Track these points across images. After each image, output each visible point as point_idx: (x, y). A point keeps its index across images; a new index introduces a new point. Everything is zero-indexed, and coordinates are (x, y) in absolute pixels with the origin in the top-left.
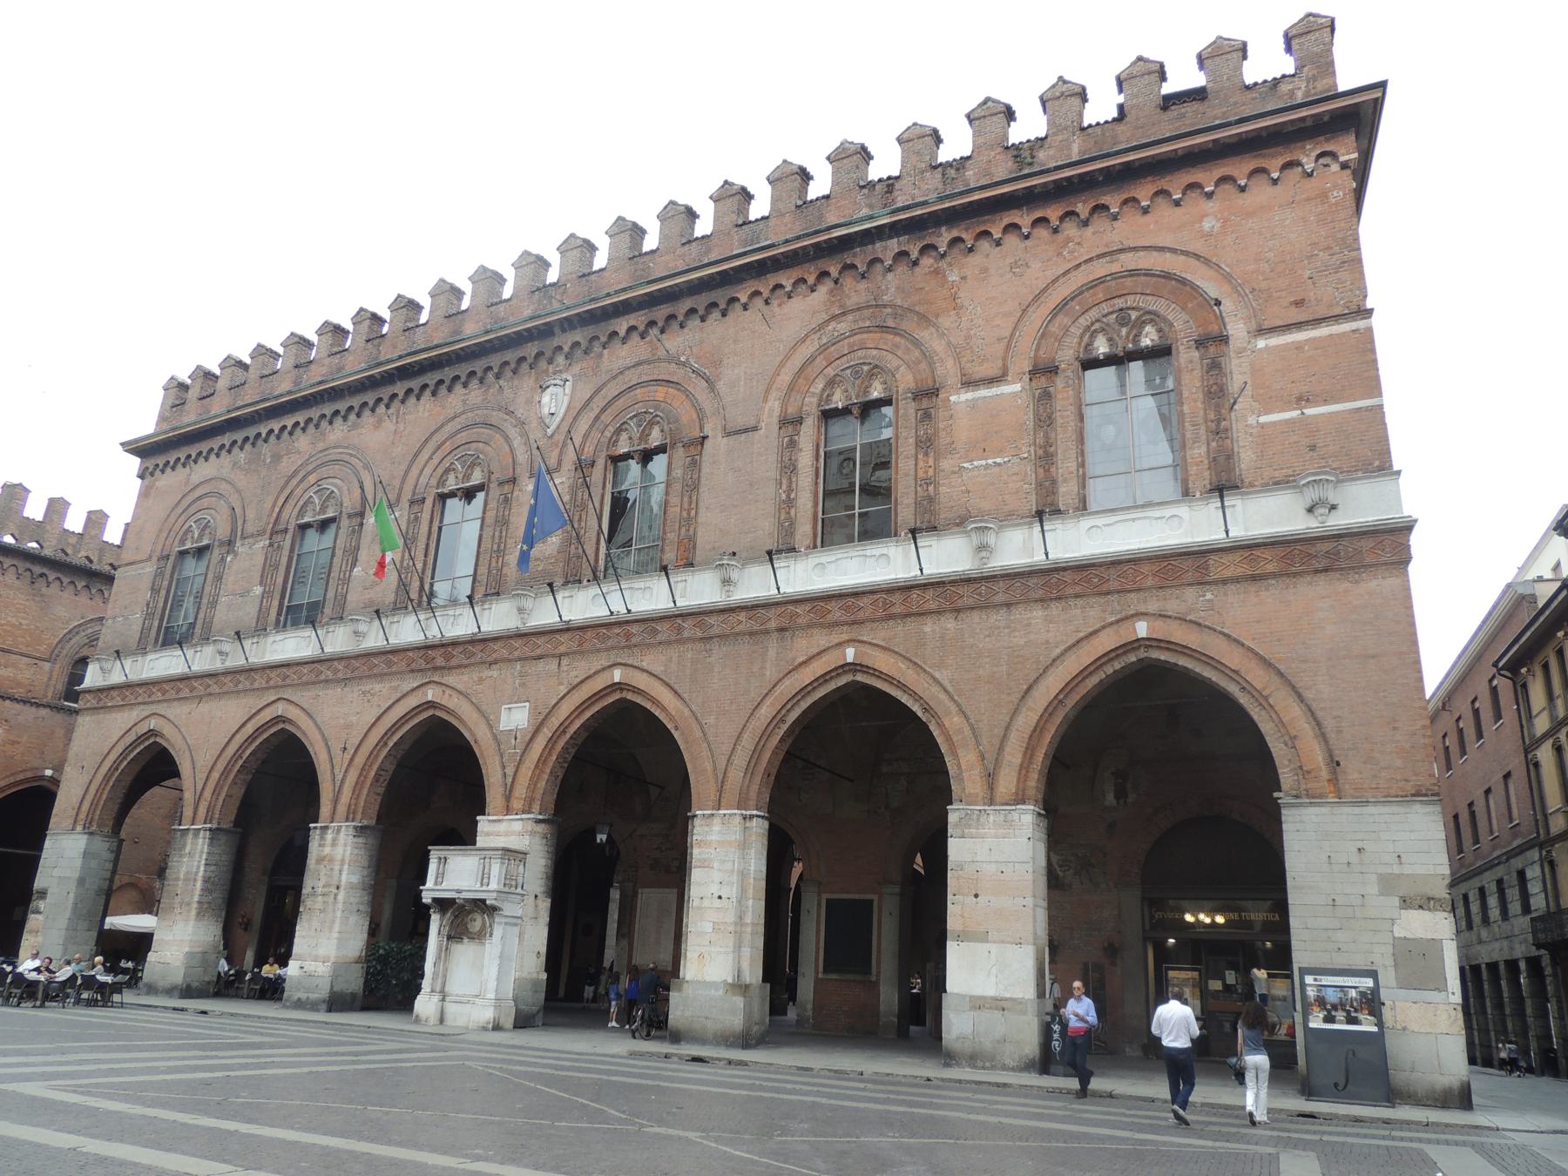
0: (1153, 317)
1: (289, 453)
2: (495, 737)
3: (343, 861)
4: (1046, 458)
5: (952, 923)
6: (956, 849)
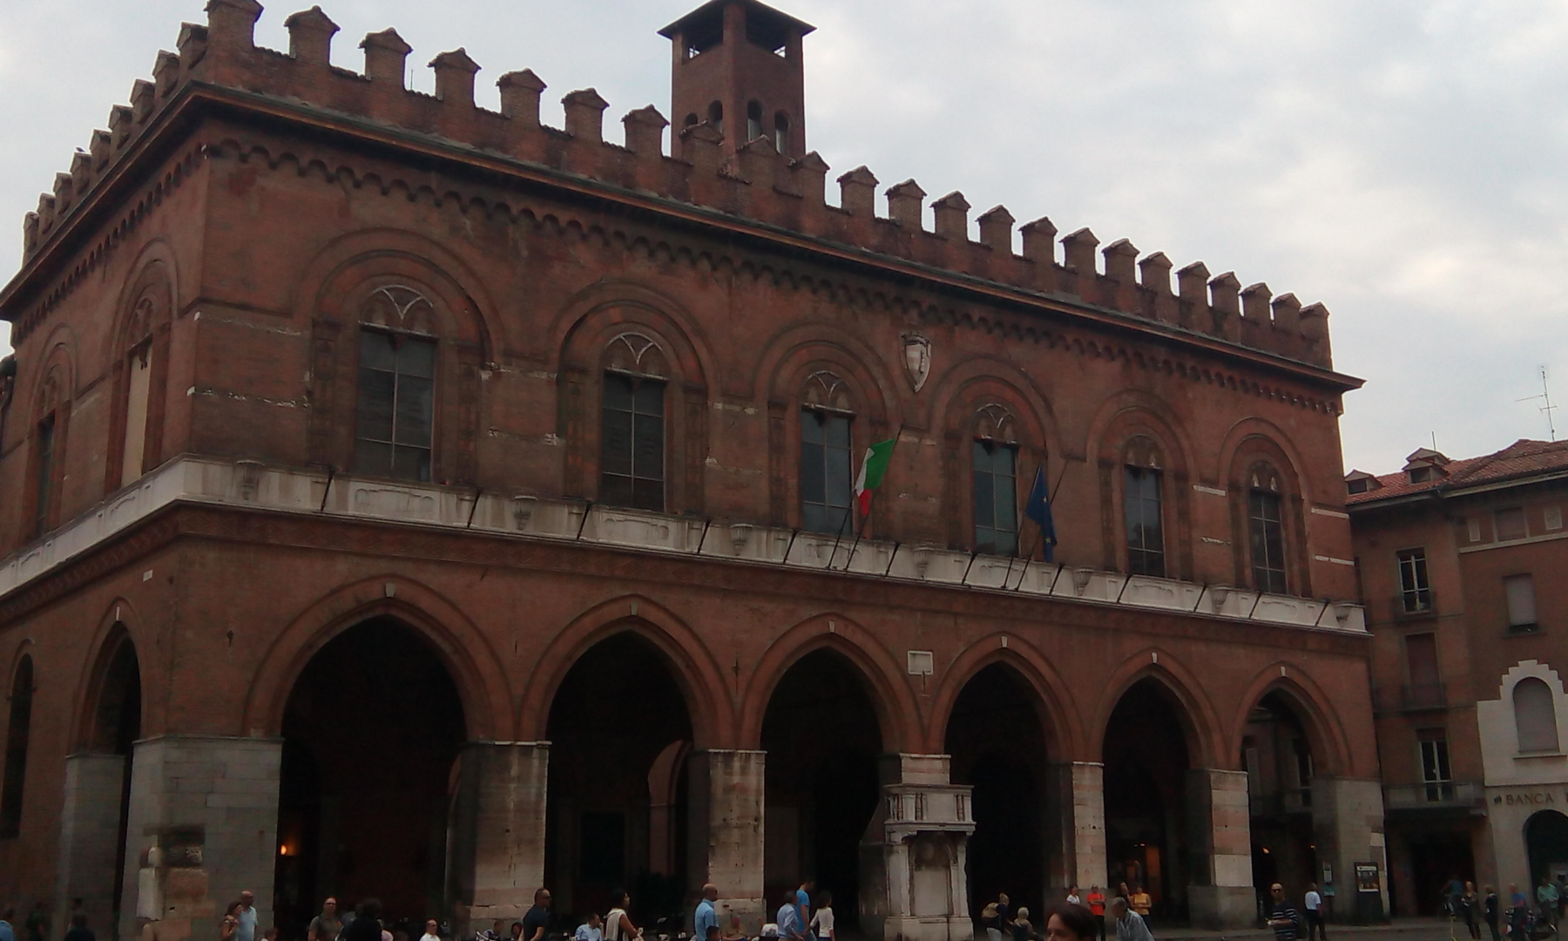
0: (1275, 474)
3: (758, 791)
4: (1237, 548)
5: (1217, 843)
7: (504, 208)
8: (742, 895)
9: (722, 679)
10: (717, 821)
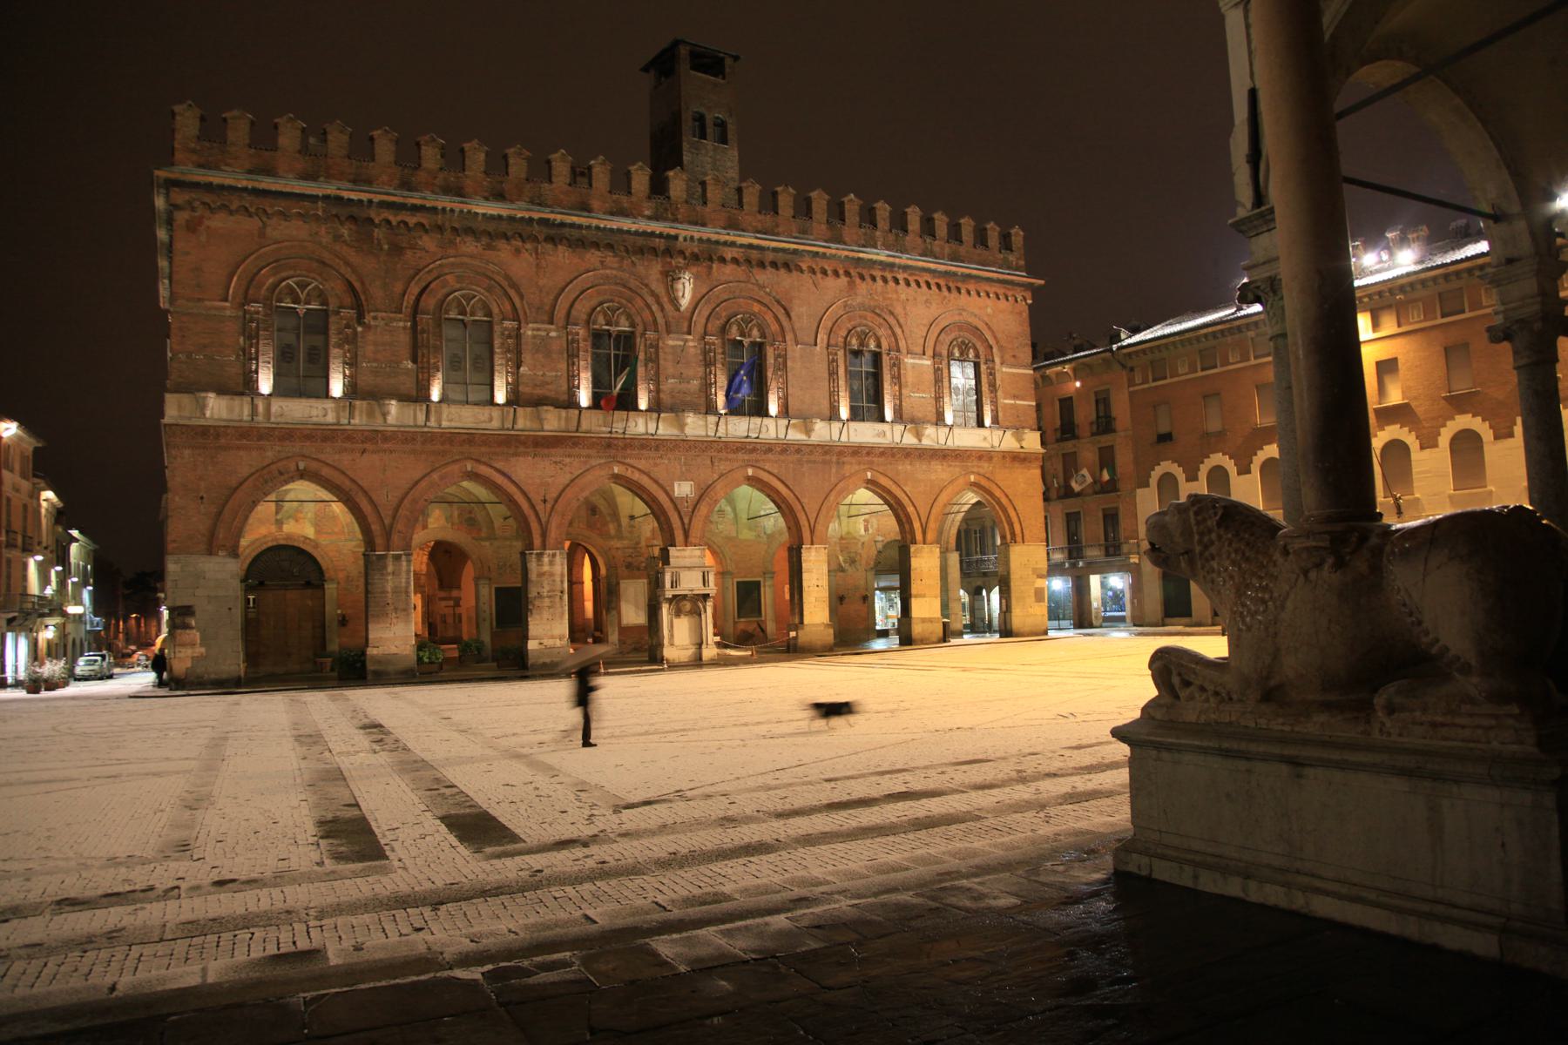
1: (413, 247)
2: (672, 500)
5: (914, 591)
6: (914, 563)
7: (371, 220)
8: (552, 637)
9: (533, 507)
10: (533, 593)
